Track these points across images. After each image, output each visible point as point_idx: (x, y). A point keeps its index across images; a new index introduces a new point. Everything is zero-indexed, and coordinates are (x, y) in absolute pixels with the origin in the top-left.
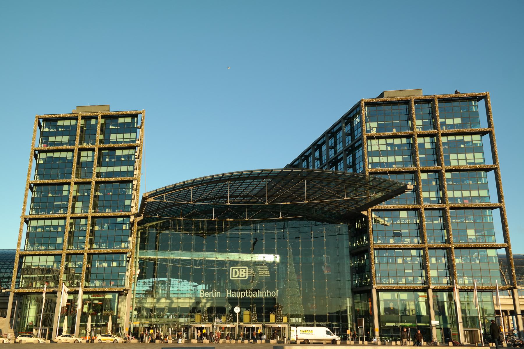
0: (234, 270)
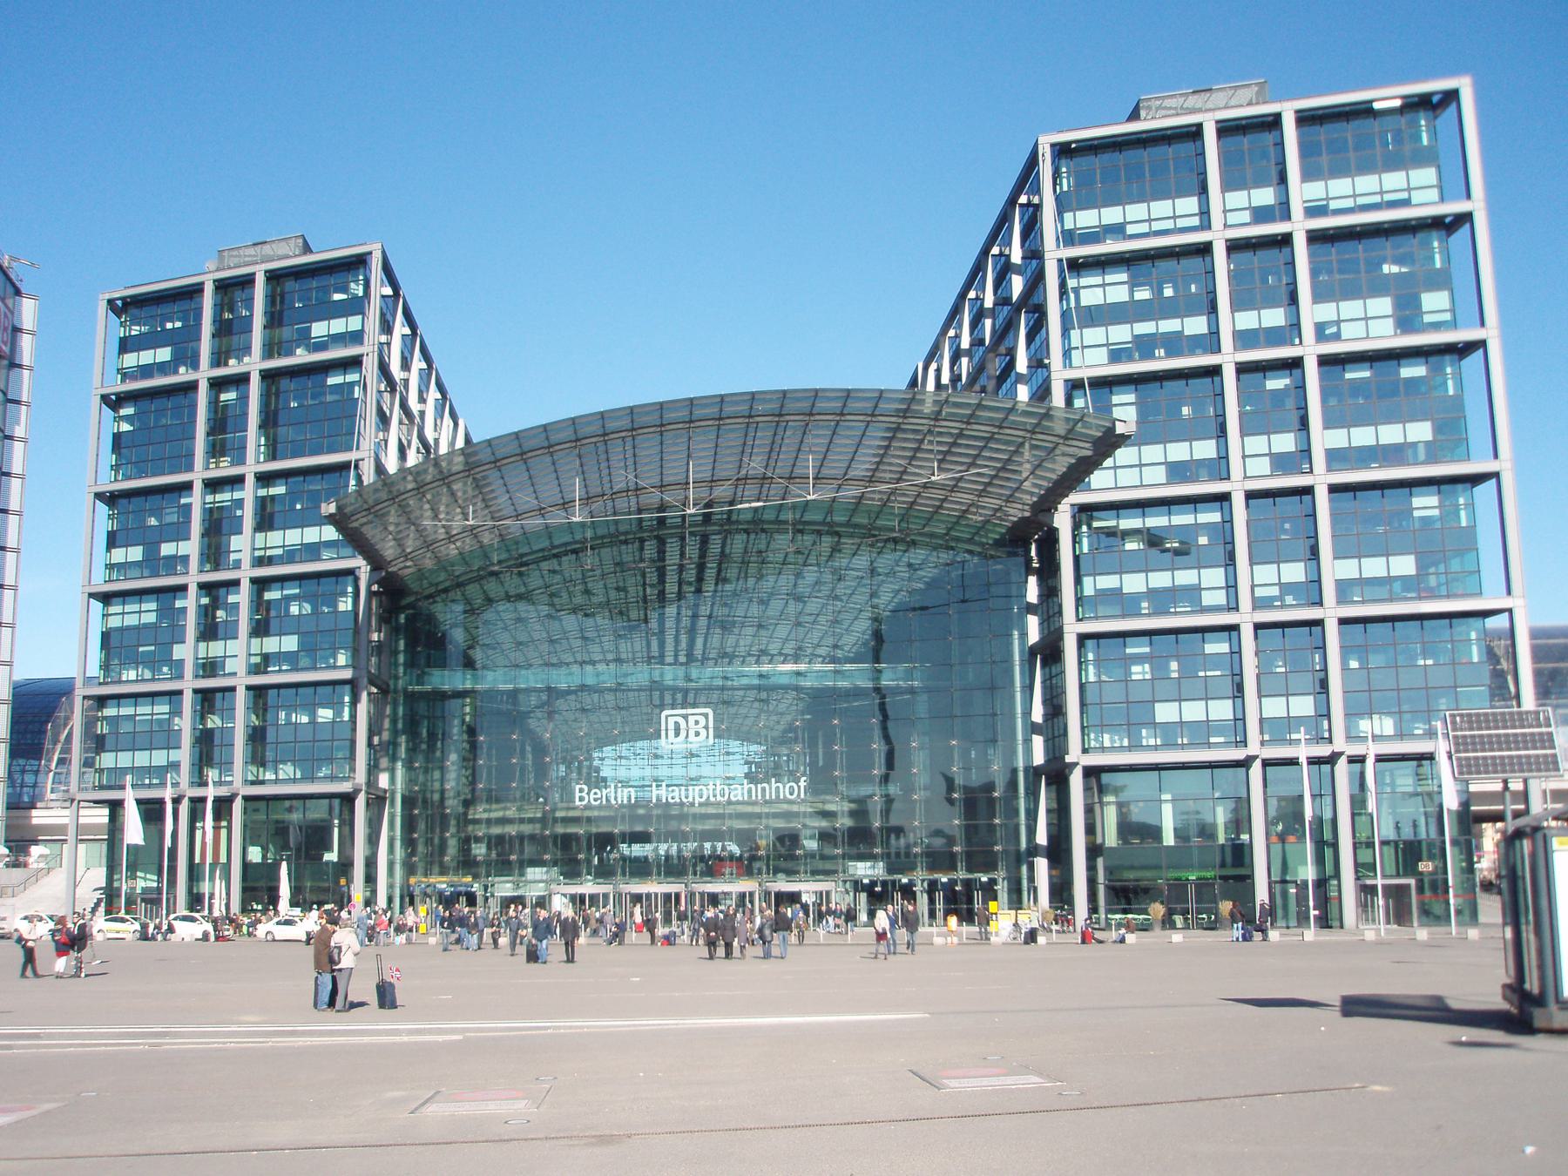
0: (671, 721)
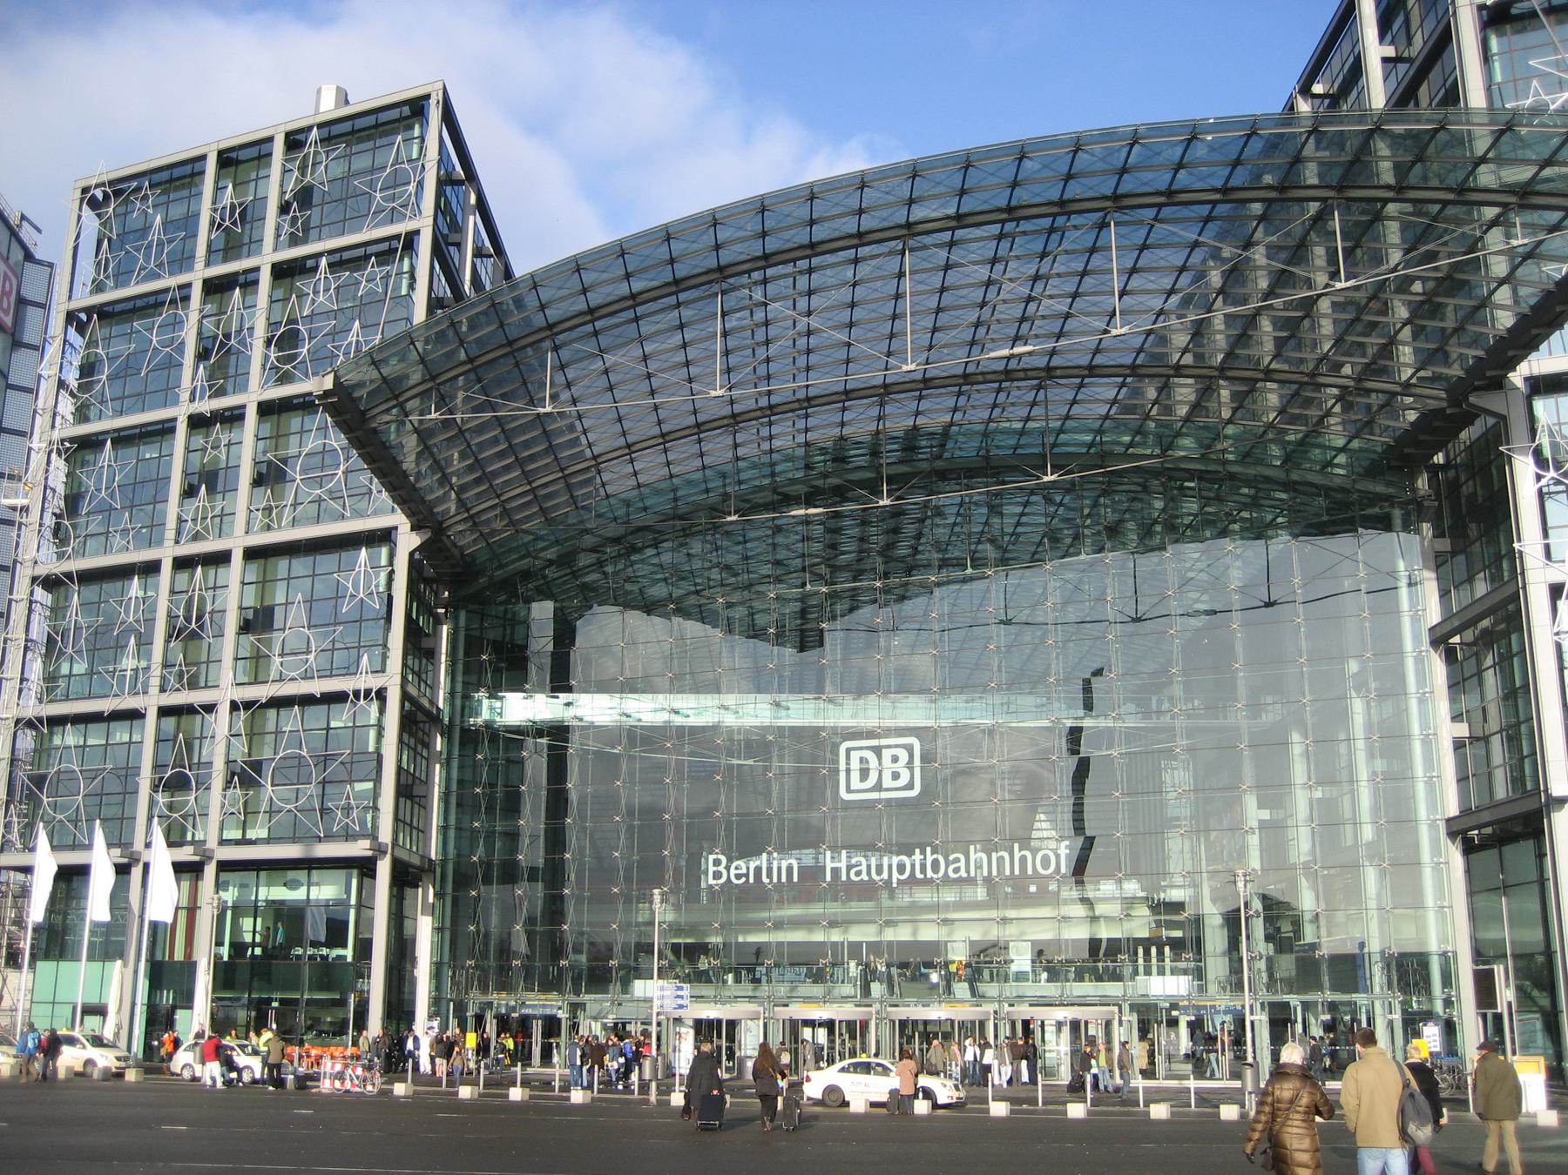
0: (855, 756)
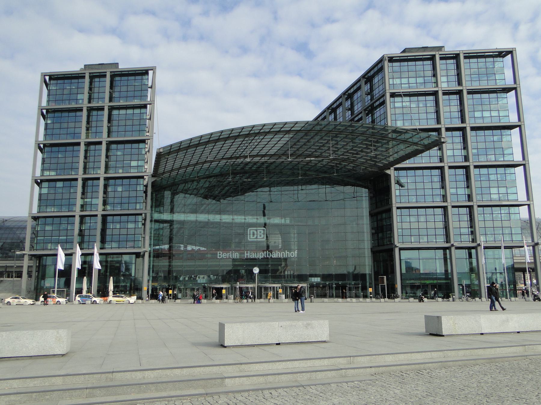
0: (252, 231)
